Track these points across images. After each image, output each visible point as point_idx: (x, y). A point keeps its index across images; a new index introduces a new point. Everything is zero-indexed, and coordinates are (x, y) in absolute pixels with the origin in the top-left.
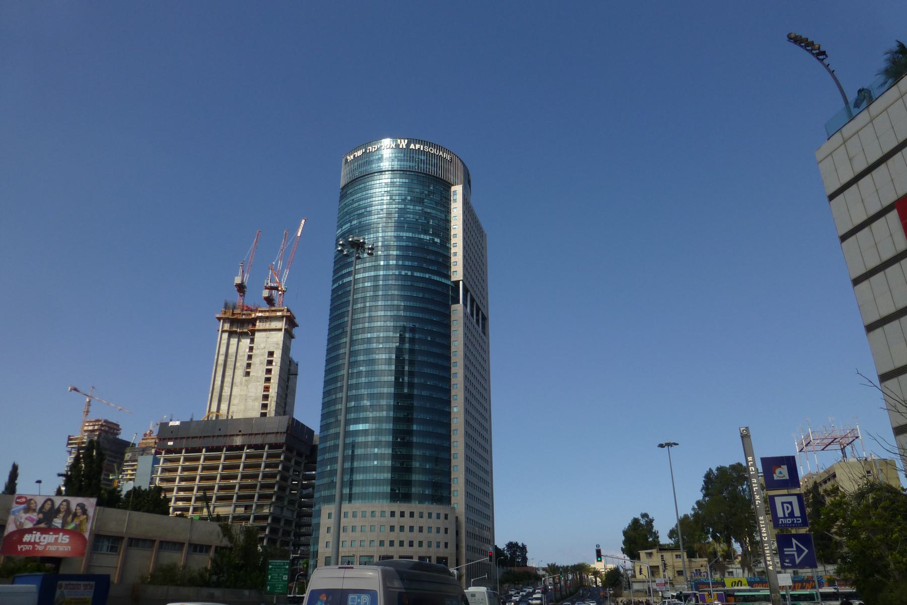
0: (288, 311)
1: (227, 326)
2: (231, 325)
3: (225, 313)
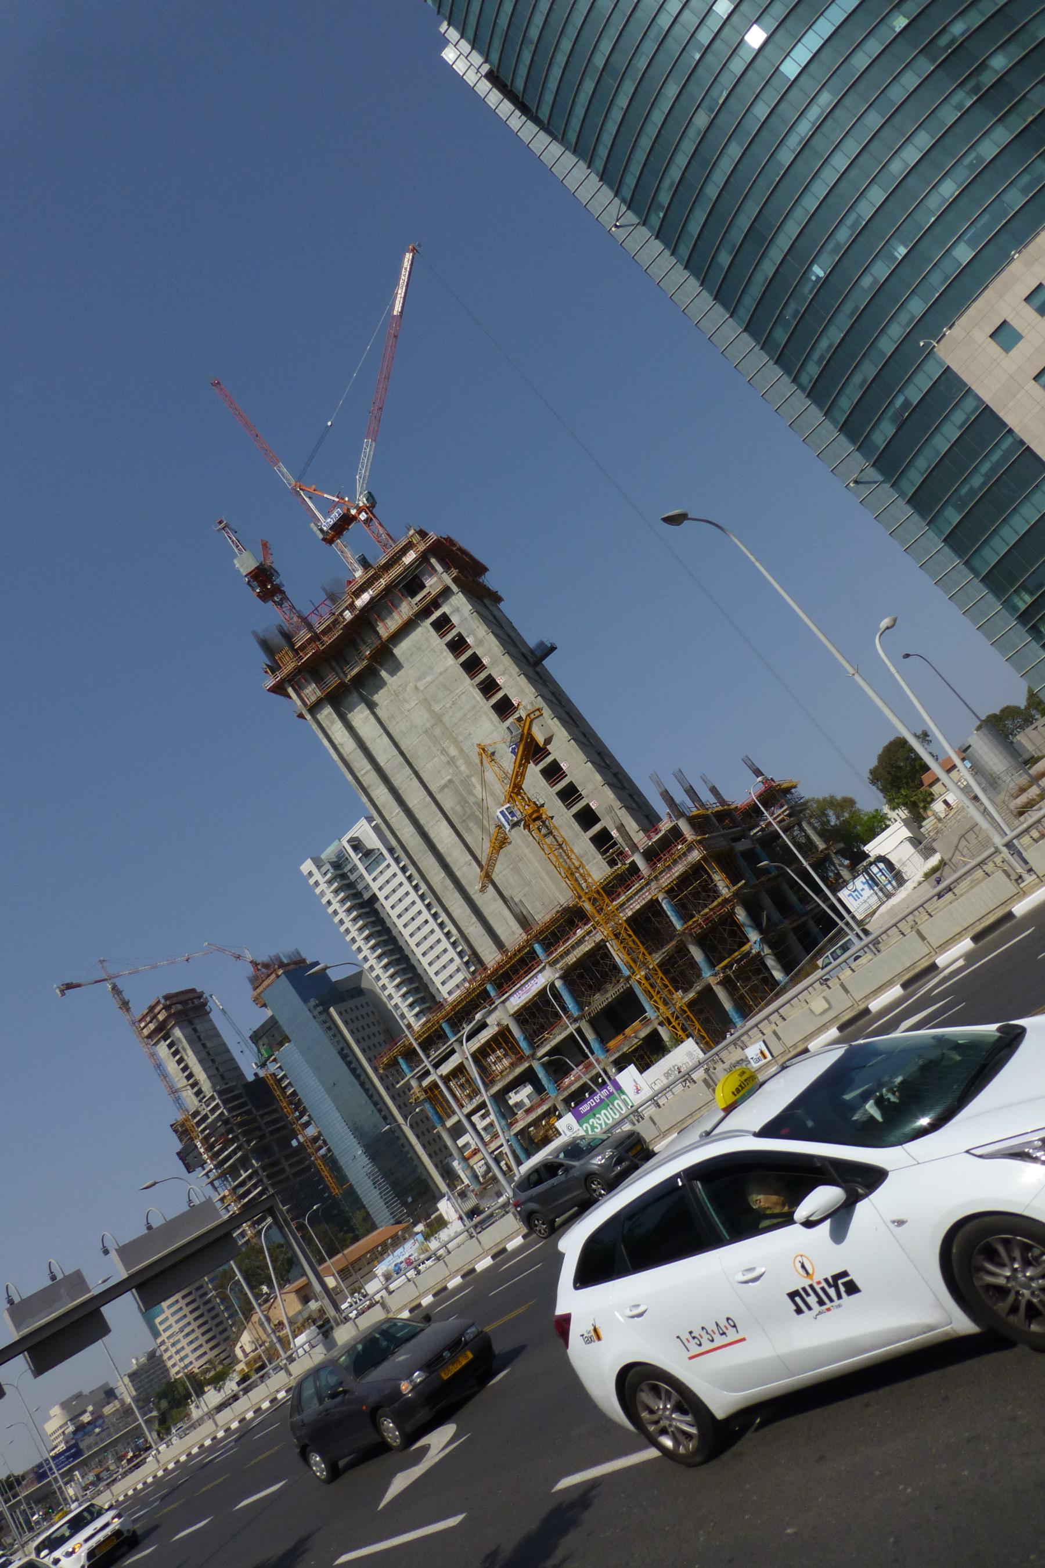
0: (423, 534)
1: (312, 692)
2: (318, 678)
3: (273, 669)
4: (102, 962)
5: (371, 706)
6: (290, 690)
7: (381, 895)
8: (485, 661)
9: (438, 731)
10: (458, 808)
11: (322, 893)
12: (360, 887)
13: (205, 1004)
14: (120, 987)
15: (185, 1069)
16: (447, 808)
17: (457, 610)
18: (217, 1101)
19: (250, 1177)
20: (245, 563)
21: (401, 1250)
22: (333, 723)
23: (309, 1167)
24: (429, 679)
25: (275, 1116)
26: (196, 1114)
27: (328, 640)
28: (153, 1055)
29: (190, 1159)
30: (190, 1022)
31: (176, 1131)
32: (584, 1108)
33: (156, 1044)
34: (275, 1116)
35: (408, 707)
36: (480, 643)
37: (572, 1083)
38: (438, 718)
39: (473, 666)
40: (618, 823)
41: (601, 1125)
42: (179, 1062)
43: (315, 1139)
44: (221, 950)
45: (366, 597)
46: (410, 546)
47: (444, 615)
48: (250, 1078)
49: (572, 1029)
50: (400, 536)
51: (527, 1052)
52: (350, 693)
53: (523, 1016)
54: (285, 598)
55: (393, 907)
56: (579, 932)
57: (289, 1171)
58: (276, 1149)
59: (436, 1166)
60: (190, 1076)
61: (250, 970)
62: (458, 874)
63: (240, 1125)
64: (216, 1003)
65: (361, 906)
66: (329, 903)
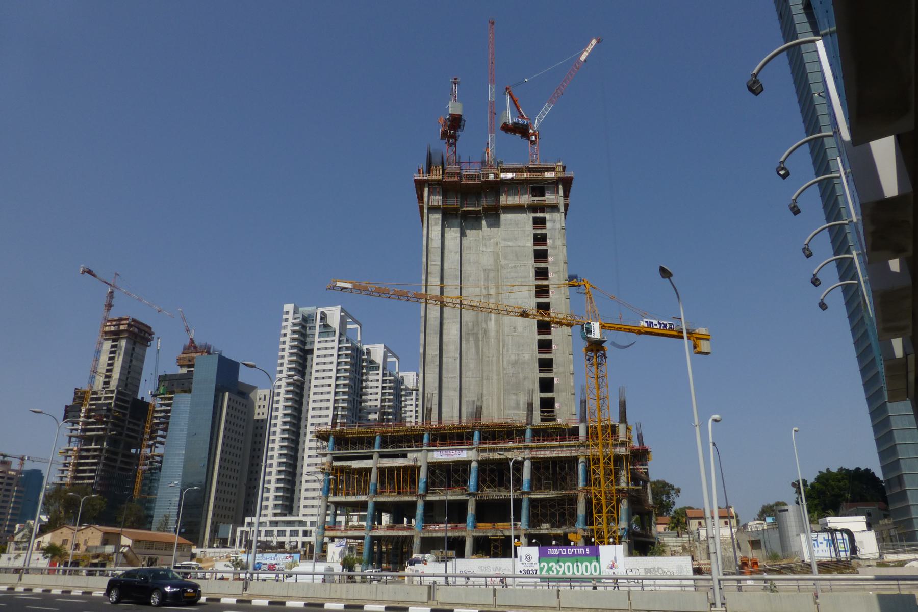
0: (564, 168)
1: (437, 200)
2: (445, 195)
4: (117, 274)
5: (463, 234)
6: (426, 190)
7: (316, 353)
8: (550, 259)
9: (492, 275)
10: (470, 324)
11: (285, 327)
12: (308, 340)
13: (149, 340)
14: (115, 295)
15: (109, 365)
16: (464, 319)
17: (554, 221)
18: (114, 395)
19: (95, 450)
20: (454, 108)
21: (273, 555)
22: (436, 224)
23: (130, 470)
24: (510, 244)
25: (136, 428)
26: (95, 393)
27: (464, 181)
28: (101, 344)
29: (71, 414)
30: (135, 343)
31: (76, 394)
32: (553, 551)
33: (106, 339)
34: (136, 428)
35: (484, 250)
36: (554, 247)
37: (435, 531)
38: (497, 268)
39: (541, 256)
40: (583, 398)
41: (558, 572)
42: (110, 359)
43: (161, 456)
44: (184, 319)
45: (509, 176)
46: (553, 169)
47: (545, 218)
48: (139, 398)
49: (512, 495)
50: (552, 162)
51: (421, 492)
52: (457, 218)
53: (433, 467)
54: (455, 144)
55: (317, 364)
56: (511, 444)
57: (118, 464)
58: (122, 446)
59: (212, 523)
60: (110, 371)
61: (188, 343)
62: (444, 360)
63: (115, 417)
64: (157, 344)
65: (301, 350)
66: (285, 335)
